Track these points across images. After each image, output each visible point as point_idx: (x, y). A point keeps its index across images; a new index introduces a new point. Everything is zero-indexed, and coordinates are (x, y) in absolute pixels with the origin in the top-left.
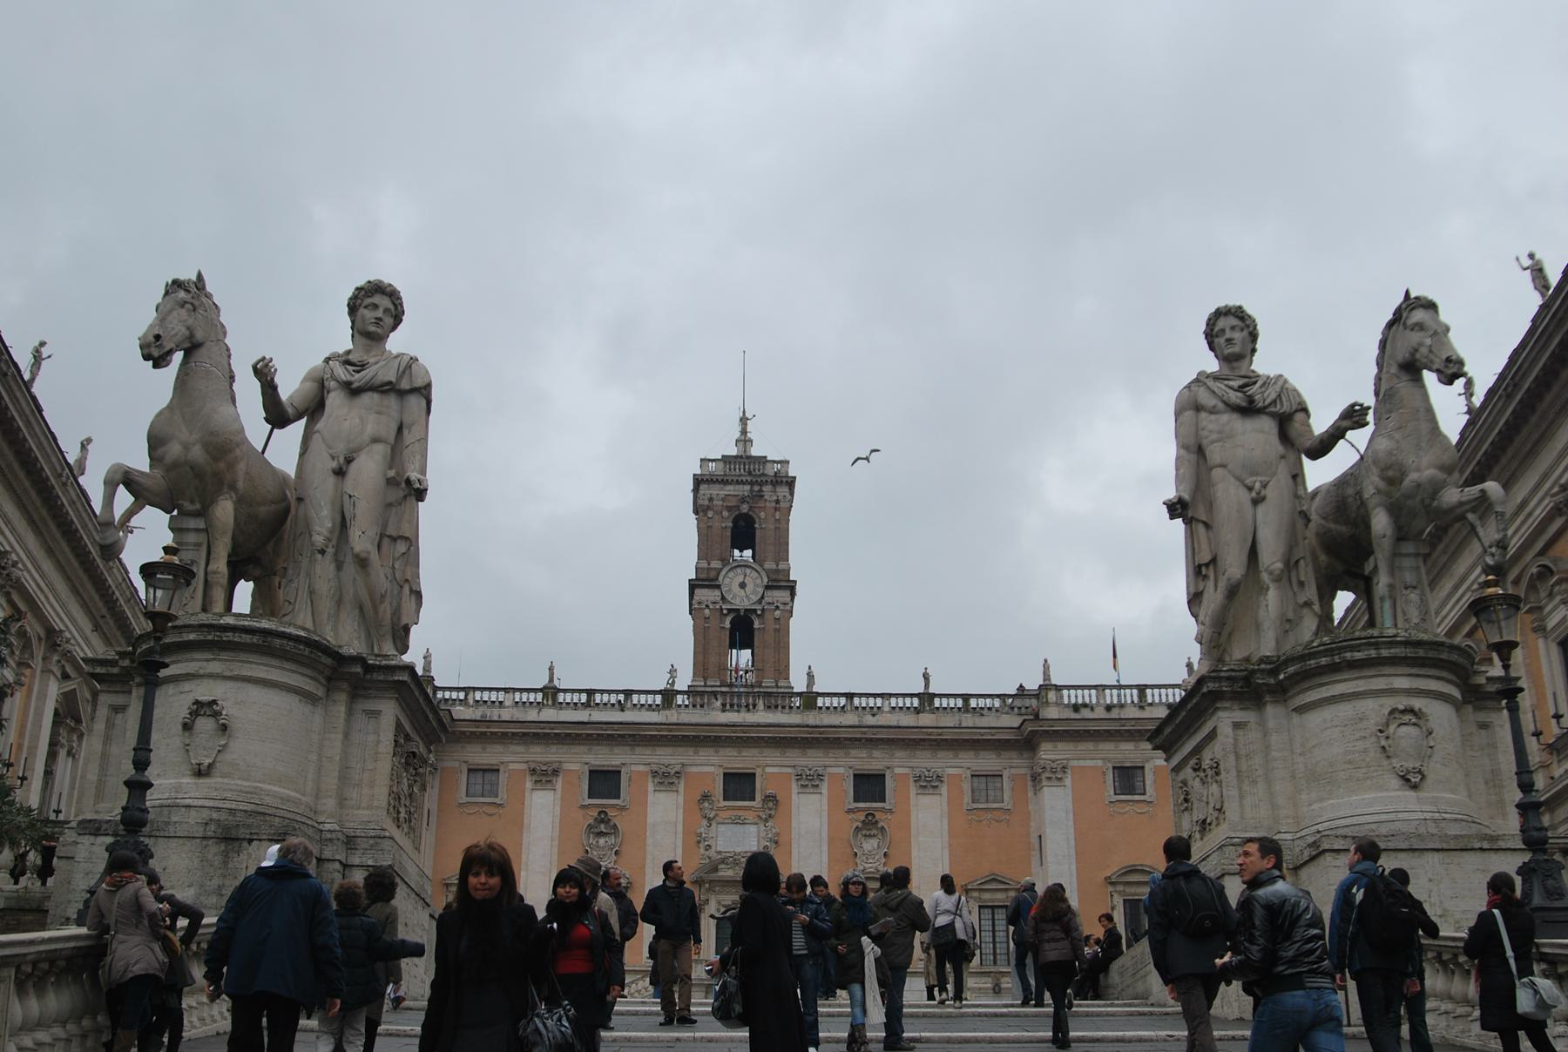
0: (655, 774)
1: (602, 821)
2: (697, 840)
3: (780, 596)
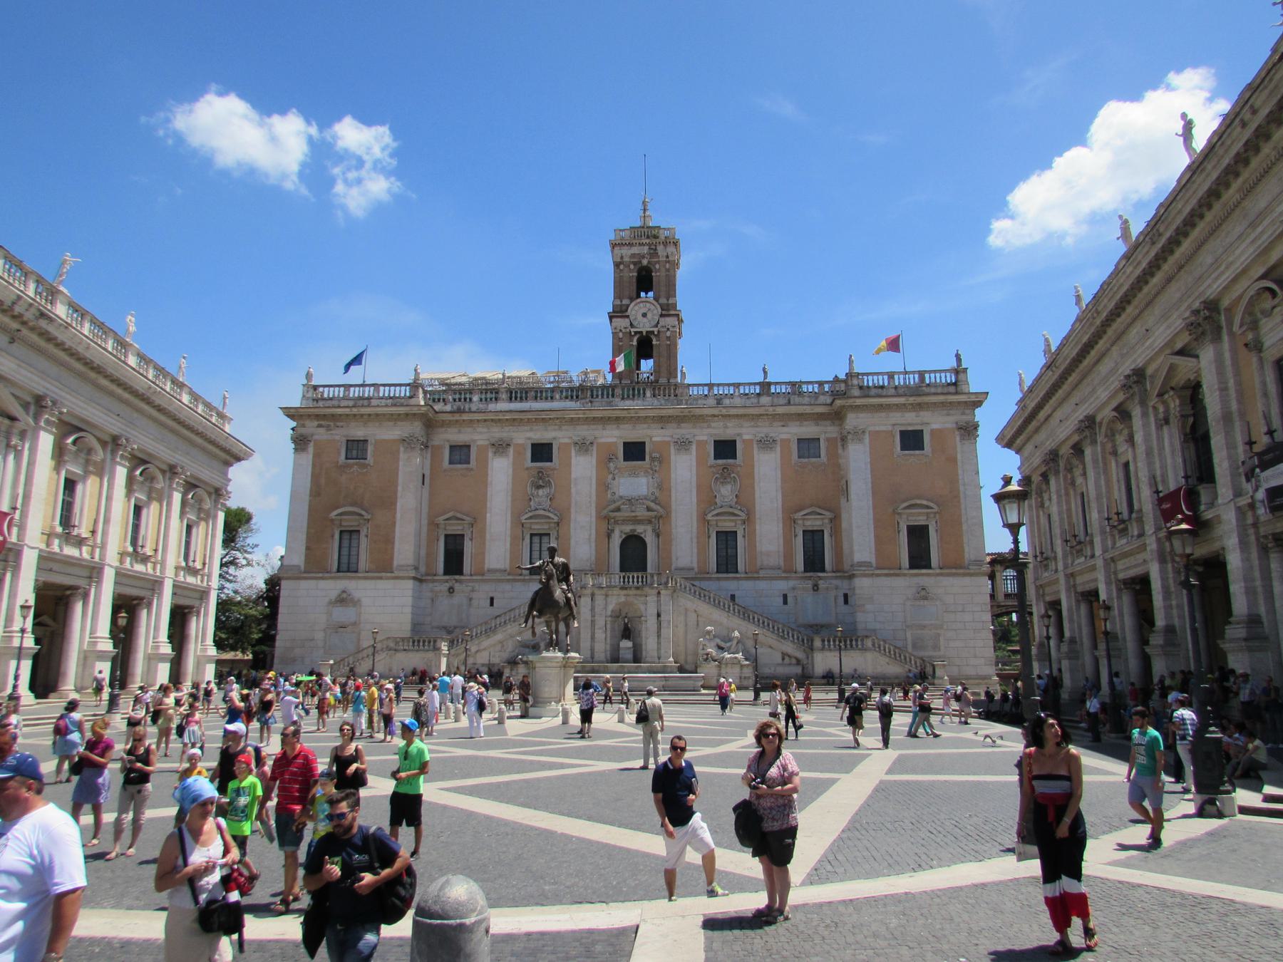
2: (603, 486)
3: (670, 321)
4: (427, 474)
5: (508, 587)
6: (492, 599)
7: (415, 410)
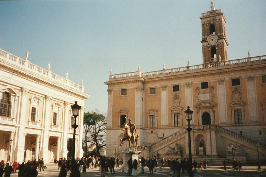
0: (186, 85)
1: (176, 96)
2: (196, 98)
4: (144, 97)
5: (168, 130)
6: (164, 134)
7: (138, 79)
